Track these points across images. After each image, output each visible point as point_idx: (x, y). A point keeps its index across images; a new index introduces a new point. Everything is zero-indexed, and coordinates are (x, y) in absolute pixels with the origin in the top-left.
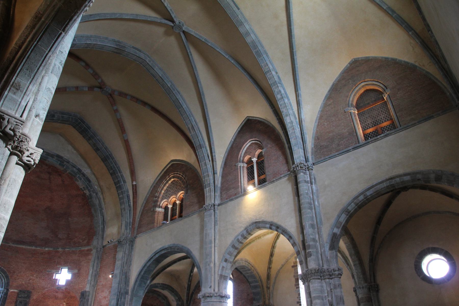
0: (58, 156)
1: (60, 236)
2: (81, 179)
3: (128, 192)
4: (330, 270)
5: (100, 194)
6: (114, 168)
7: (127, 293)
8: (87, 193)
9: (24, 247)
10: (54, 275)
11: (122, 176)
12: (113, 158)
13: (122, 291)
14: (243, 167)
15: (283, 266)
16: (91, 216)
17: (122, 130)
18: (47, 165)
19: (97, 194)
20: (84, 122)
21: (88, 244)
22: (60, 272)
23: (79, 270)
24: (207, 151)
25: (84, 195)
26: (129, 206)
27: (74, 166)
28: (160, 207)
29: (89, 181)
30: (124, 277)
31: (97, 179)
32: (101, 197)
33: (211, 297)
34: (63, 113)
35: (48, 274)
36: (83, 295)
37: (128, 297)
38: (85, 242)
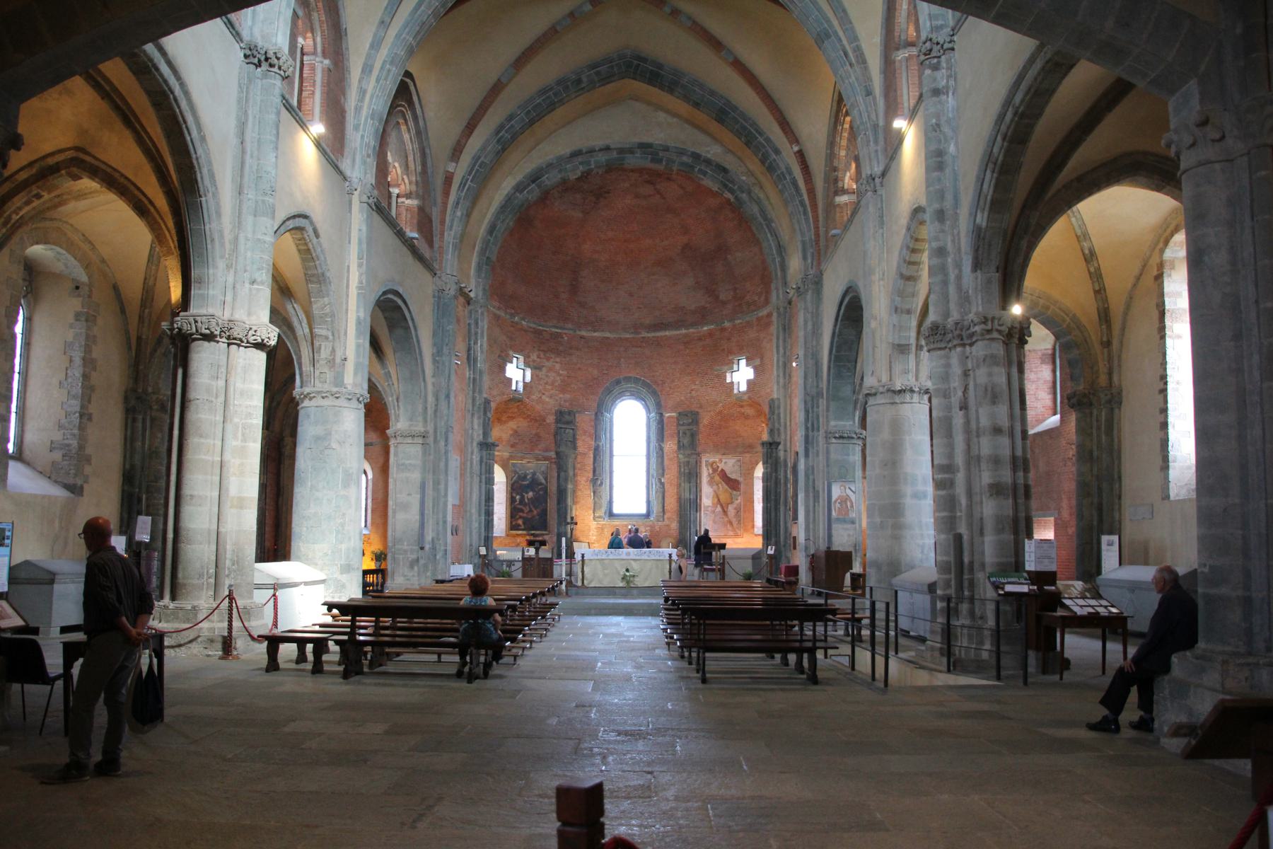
0: (644, 146)
1: (722, 297)
2: (705, 174)
3: (790, 172)
4: (966, 323)
5: (756, 190)
6: (744, 128)
7: (819, 394)
8: (728, 195)
9: (667, 333)
10: (728, 375)
11: (768, 140)
12: (735, 108)
13: (814, 391)
14: (907, 59)
15: (1138, 278)
16: (757, 242)
17: (716, 44)
18: (632, 171)
19: (749, 192)
20: (645, 60)
21: (767, 302)
22: (735, 367)
23: (762, 359)
24: (840, 40)
25: (728, 201)
26: (802, 203)
27: (682, 152)
28: (844, 191)
29: (725, 170)
30: (811, 362)
31: (739, 158)
32: (762, 196)
33: (875, 394)
34: (594, 66)
35: (718, 376)
36: (773, 405)
37: (823, 403)
38: (763, 298)
